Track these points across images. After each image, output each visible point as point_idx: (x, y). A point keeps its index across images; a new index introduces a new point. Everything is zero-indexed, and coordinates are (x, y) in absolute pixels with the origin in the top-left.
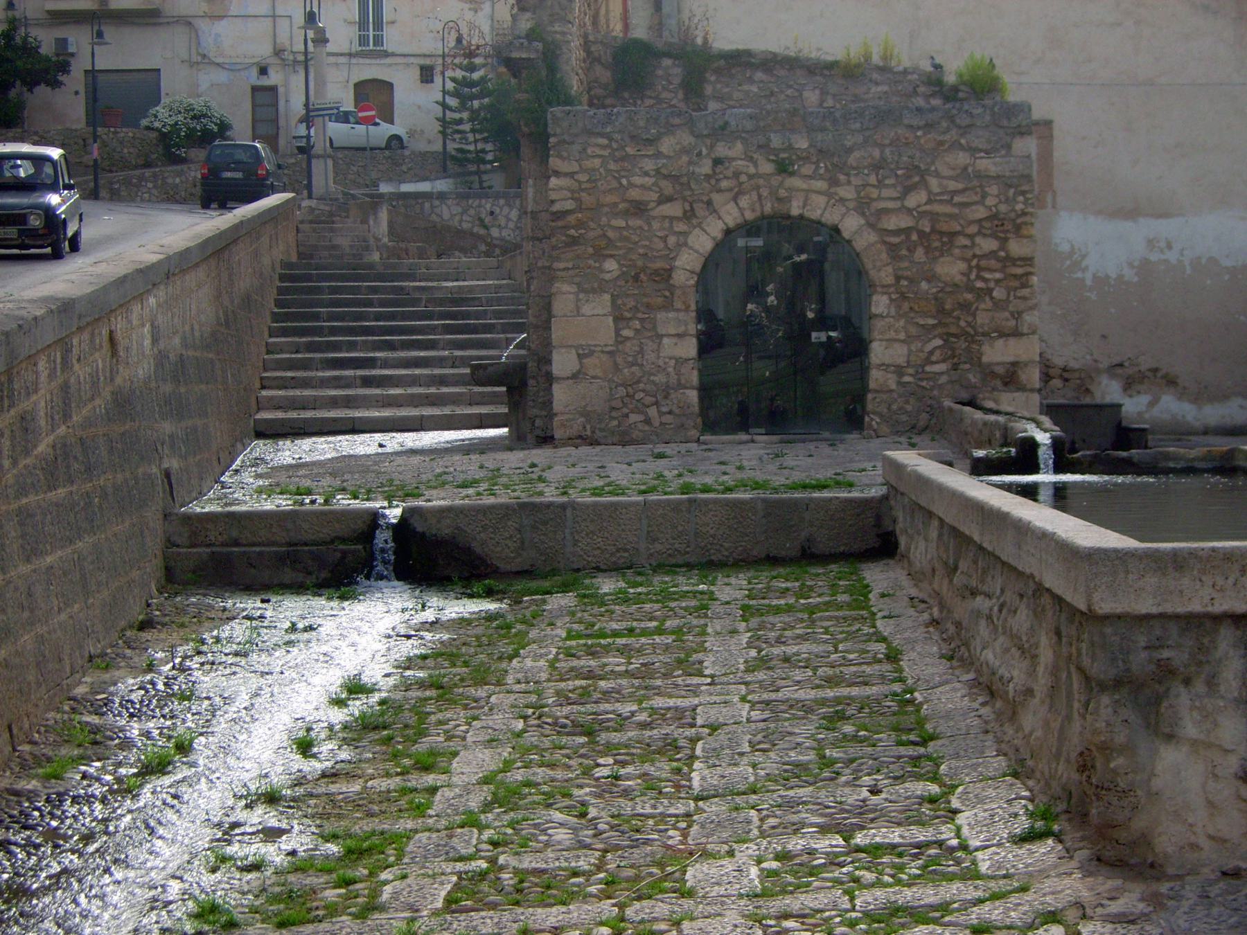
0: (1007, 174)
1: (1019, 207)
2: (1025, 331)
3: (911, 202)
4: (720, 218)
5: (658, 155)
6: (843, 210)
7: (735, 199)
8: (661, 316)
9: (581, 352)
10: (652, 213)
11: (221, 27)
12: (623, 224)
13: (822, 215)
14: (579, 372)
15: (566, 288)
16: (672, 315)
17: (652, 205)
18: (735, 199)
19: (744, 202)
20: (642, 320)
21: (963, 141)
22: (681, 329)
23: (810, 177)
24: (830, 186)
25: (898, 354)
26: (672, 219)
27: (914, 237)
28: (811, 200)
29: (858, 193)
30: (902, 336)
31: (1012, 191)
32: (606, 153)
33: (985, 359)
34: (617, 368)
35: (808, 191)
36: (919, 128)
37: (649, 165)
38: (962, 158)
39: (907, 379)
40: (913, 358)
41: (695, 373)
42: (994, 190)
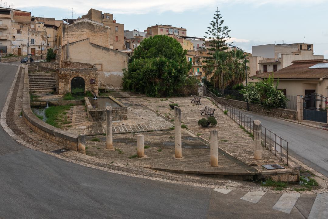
11: (14, 41)
19: (75, 76)
25: (87, 87)
28: (80, 75)
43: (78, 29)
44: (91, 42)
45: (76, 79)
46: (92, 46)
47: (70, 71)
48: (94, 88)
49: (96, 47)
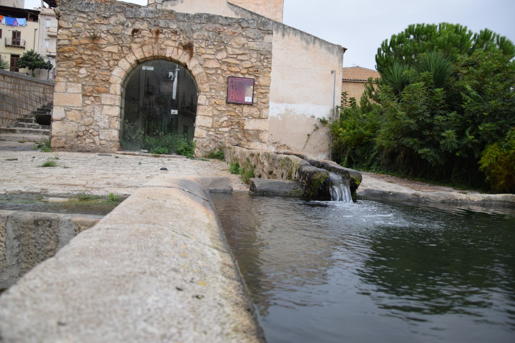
1: (265, 64)
2: (263, 117)
3: (220, 56)
4: (134, 55)
8: (103, 96)
9: (66, 109)
10: (103, 50)
12: (90, 53)
14: (64, 118)
15: (61, 79)
16: (108, 96)
18: (141, 47)
19: (145, 49)
20: (95, 97)
21: (244, 34)
22: (112, 103)
25: (208, 122)
26: (112, 53)
33: (245, 128)
34: (82, 117)
36: (225, 26)
37: (104, 28)
38: (243, 40)
39: (211, 133)
40: (214, 124)
41: (117, 122)
45: (152, 69)
48: (245, 132)
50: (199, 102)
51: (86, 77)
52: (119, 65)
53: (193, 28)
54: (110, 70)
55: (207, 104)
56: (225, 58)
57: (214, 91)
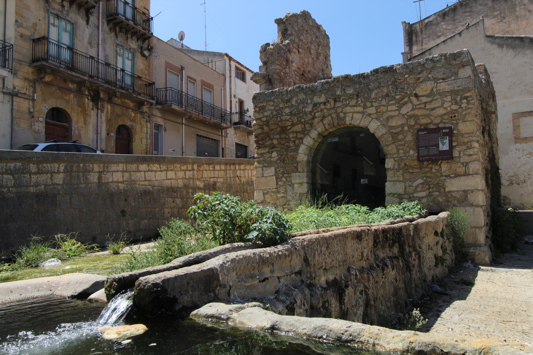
0: (456, 89)
2: (471, 173)
3: (404, 110)
5: (292, 106)
6: (370, 119)
7: (322, 120)
8: (293, 175)
13: (360, 123)
16: (297, 174)
17: (289, 128)
19: (326, 121)
20: (286, 178)
23: (354, 106)
24: (364, 108)
26: (297, 132)
27: (406, 128)
29: (377, 110)
30: (401, 179)
31: (458, 98)
32: (273, 108)
33: (447, 190)
35: (353, 113)
37: (287, 111)
42: (449, 98)
43: (454, 25)
44: (488, 34)
45: (336, 140)
46: (495, 46)
47: (302, 96)
48: (447, 195)
49: (513, 47)
50: (386, 166)
51: (278, 160)
52: (304, 142)
53: (370, 87)
54: (296, 150)
55: (396, 167)
56: (411, 111)
57: (402, 152)
